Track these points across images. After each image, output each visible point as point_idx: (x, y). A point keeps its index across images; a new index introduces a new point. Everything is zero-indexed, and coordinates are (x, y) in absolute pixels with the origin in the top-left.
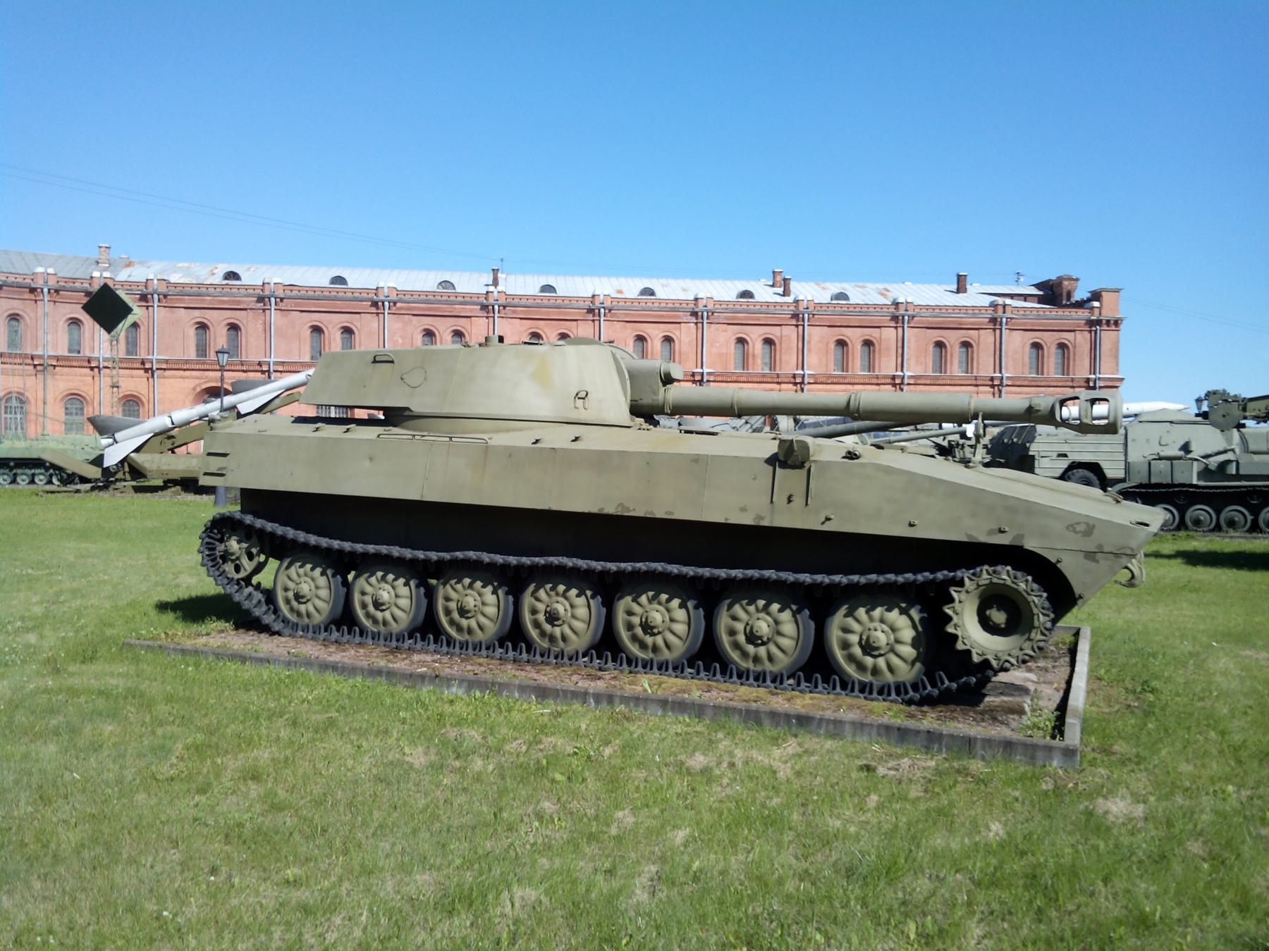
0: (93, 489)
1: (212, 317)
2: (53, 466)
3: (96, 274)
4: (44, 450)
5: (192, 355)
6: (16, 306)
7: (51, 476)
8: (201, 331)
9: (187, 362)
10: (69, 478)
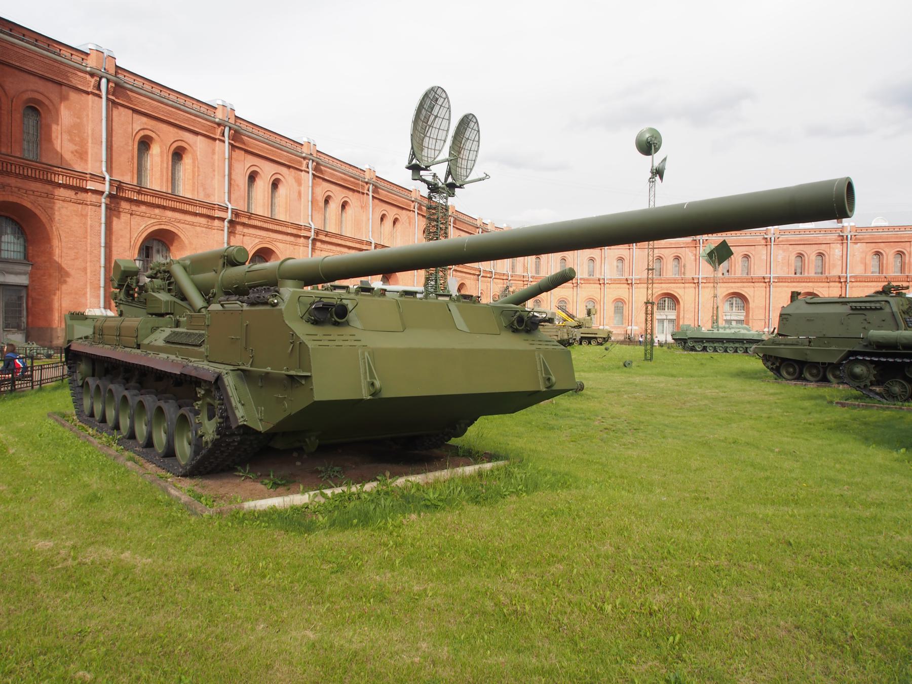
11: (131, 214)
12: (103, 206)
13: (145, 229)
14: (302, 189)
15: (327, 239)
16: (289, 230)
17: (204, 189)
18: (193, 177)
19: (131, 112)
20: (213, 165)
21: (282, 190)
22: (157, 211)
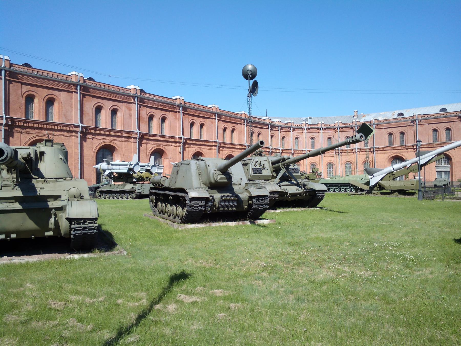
0: (366, 194)
1: (394, 130)
2: (352, 185)
3: (354, 121)
4: (349, 180)
5: (387, 145)
6: (330, 134)
7: (352, 189)
8: (390, 136)
9: (385, 147)
10: (359, 190)
11: (21, 133)
12: (3, 130)
13: (30, 139)
14: (132, 112)
15: (150, 138)
16: (123, 135)
17: (66, 117)
18: (59, 112)
19: (20, 84)
20: (72, 104)
21: (119, 114)
22: (37, 131)
